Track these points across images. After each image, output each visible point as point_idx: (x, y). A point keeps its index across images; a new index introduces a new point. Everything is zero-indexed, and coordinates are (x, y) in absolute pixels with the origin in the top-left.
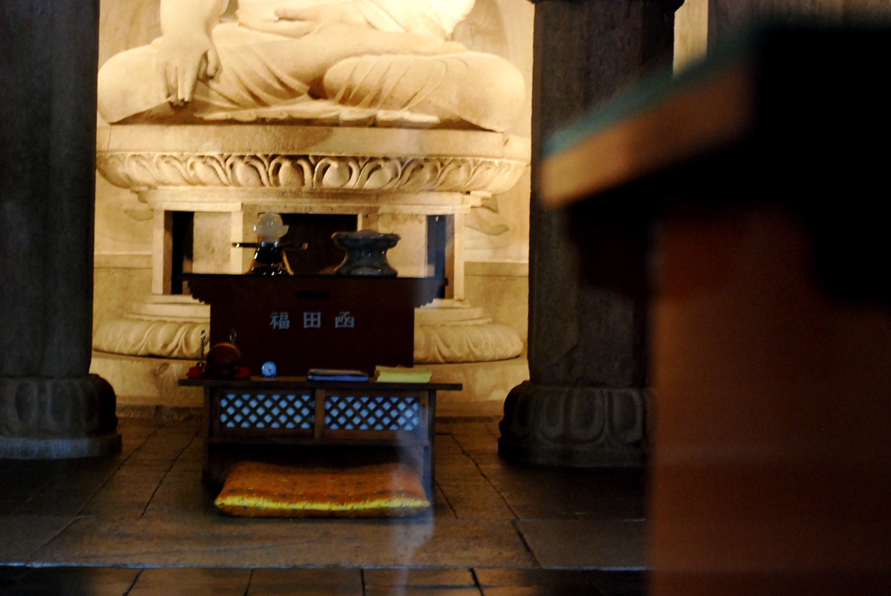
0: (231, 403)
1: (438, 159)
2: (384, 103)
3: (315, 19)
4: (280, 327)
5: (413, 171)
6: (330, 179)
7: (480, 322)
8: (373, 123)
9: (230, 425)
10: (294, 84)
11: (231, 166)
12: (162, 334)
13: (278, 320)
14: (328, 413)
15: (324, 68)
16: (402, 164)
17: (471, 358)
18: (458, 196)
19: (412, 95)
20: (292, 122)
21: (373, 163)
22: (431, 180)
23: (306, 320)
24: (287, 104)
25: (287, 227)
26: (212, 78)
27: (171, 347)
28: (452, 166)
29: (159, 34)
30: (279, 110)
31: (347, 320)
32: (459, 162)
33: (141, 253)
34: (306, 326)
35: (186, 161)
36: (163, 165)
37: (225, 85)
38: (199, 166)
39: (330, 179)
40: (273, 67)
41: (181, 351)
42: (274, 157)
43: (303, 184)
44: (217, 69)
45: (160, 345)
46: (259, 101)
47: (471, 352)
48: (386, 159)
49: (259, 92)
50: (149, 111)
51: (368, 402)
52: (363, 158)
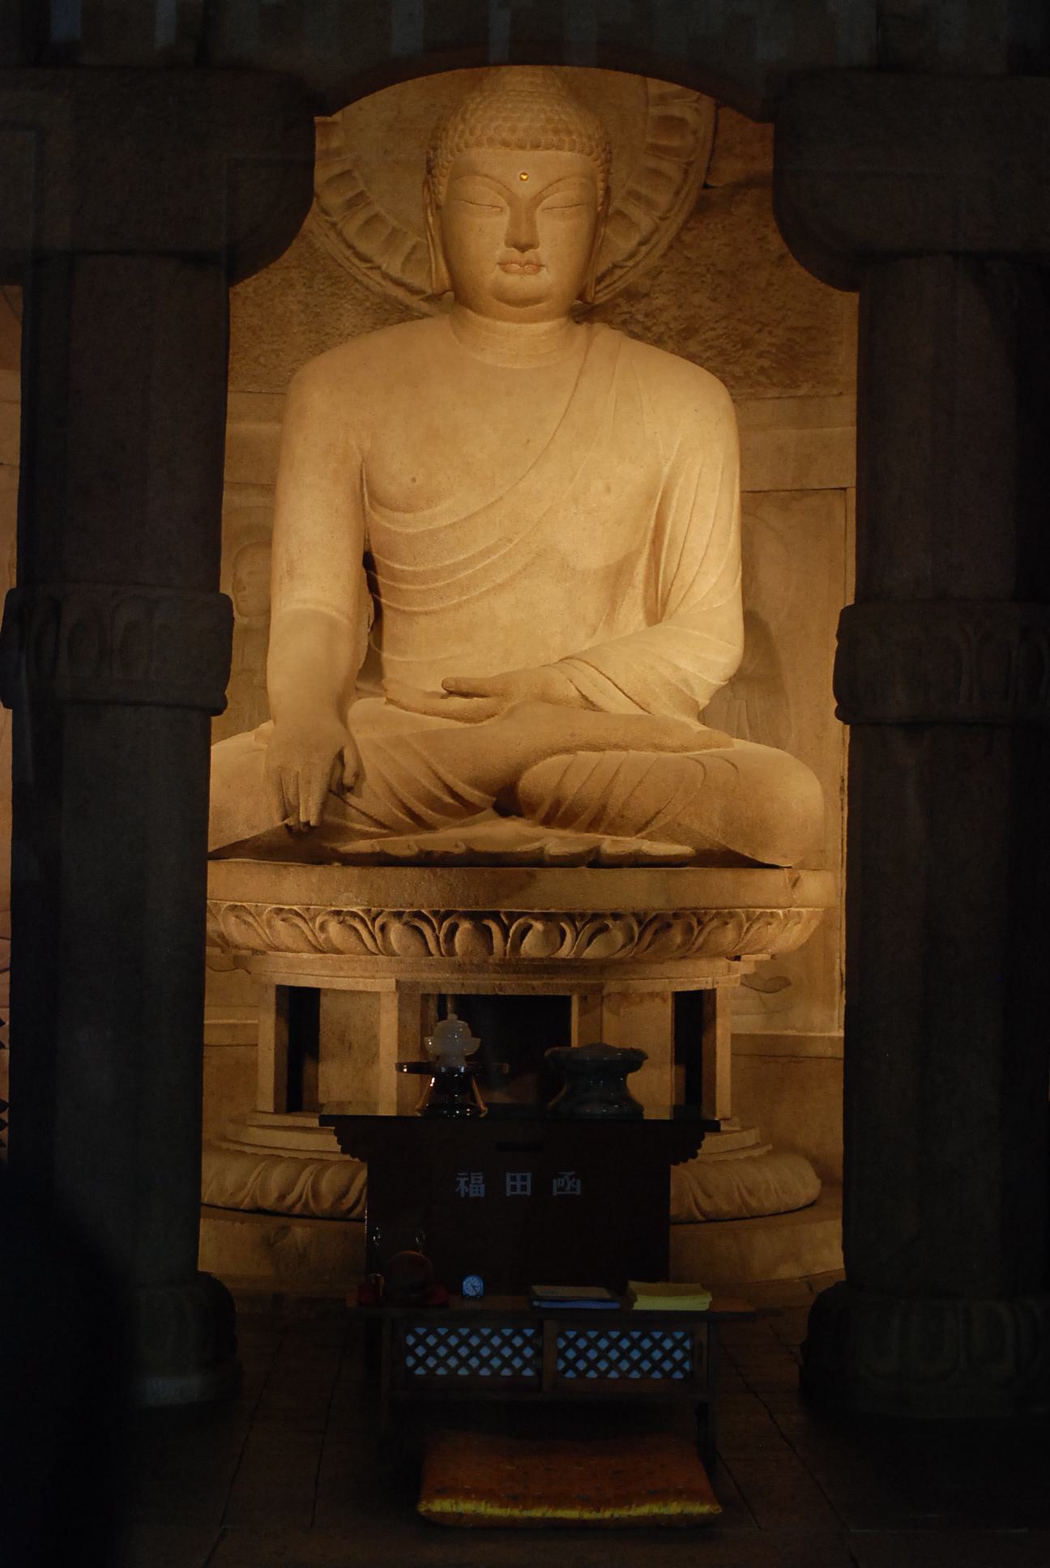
0: (421, 1340)
1: (694, 914)
2: (611, 825)
3: (503, 694)
4: (472, 1195)
5: (656, 932)
6: (530, 946)
7: (756, 1153)
8: (595, 860)
9: (420, 1371)
10: (473, 794)
11: (383, 928)
12: (277, 1178)
13: (467, 1183)
14: (561, 1354)
15: (518, 772)
16: (640, 923)
17: (745, 1213)
18: (723, 963)
19: (652, 813)
20: (473, 859)
21: (596, 922)
22: (684, 944)
23: (509, 1183)
24: (463, 825)
25: (479, 1040)
26: (350, 789)
27: (290, 1199)
28: (715, 923)
29: (266, 715)
30: (451, 837)
31: (570, 1183)
32: (725, 916)
33: (225, 1021)
34: (509, 1193)
35: (313, 919)
36: (278, 924)
37: (370, 800)
38: (333, 927)
39: (530, 946)
40: (442, 770)
41: (306, 1204)
42: (448, 914)
43: (490, 950)
44: (359, 775)
45: (275, 1195)
46: (421, 823)
47: (745, 1203)
48: (616, 916)
49: (420, 809)
50: (256, 838)
51: (619, 1339)
52: (582, 916)
